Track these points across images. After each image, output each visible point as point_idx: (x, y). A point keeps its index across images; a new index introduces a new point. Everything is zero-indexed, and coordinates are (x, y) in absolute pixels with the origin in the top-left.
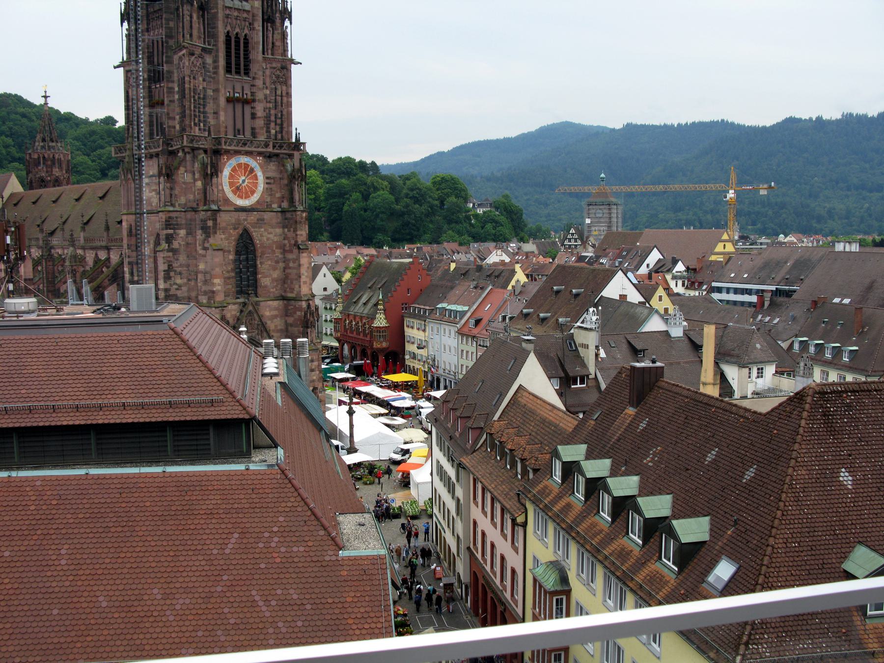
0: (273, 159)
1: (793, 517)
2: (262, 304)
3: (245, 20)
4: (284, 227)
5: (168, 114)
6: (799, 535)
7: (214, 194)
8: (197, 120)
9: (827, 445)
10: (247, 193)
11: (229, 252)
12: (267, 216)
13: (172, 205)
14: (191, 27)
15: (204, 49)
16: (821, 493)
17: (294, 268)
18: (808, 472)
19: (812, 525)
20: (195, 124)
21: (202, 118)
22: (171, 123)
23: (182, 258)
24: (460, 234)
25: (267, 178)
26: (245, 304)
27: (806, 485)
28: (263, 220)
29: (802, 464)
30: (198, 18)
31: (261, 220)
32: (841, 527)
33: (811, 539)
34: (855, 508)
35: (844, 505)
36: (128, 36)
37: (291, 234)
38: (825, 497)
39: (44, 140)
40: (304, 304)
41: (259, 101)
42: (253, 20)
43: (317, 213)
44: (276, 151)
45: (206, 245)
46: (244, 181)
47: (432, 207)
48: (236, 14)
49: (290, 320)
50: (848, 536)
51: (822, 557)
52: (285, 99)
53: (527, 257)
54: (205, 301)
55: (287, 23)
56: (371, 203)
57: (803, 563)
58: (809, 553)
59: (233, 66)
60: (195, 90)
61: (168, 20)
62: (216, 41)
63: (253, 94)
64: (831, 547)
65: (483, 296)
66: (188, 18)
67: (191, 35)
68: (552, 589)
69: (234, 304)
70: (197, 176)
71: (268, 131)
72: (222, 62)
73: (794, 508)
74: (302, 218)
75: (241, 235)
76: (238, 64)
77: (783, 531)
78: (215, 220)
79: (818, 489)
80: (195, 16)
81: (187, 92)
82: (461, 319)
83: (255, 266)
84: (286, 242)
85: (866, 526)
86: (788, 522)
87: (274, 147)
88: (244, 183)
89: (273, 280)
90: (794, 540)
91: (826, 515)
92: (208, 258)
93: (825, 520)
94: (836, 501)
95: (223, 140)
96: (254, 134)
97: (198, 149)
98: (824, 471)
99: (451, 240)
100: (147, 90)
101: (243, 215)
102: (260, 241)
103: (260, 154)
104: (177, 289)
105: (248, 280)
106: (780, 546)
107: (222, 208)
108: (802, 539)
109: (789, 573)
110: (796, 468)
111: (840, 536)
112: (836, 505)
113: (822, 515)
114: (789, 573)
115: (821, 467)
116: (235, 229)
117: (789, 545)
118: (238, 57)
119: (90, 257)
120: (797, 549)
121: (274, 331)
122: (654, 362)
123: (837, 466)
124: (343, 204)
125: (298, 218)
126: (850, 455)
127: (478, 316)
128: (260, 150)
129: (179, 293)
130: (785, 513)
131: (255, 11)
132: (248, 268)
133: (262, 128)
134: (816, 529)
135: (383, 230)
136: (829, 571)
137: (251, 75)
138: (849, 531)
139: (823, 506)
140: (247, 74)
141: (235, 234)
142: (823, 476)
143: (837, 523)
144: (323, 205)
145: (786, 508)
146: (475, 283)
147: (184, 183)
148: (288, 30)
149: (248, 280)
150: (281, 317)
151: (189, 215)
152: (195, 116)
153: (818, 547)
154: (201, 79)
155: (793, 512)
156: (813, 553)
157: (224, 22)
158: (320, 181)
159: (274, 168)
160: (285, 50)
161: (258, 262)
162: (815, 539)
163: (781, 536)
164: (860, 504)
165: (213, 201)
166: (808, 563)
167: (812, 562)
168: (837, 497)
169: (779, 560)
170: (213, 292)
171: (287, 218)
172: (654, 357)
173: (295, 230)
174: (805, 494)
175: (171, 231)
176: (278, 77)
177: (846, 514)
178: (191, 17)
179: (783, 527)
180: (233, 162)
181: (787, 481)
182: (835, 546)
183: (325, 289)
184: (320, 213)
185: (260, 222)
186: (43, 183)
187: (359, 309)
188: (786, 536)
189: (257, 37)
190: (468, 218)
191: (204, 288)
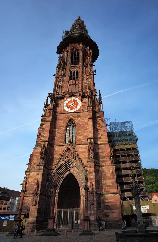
74: (90, 109)
89: (84, 137)
102: (78, 122)
116: (67, 119)
121: (83, 158)
137: (79, 78)
141: (67, 121)
161: (77, 130)
180: (69, 99)
185: (78, 116)
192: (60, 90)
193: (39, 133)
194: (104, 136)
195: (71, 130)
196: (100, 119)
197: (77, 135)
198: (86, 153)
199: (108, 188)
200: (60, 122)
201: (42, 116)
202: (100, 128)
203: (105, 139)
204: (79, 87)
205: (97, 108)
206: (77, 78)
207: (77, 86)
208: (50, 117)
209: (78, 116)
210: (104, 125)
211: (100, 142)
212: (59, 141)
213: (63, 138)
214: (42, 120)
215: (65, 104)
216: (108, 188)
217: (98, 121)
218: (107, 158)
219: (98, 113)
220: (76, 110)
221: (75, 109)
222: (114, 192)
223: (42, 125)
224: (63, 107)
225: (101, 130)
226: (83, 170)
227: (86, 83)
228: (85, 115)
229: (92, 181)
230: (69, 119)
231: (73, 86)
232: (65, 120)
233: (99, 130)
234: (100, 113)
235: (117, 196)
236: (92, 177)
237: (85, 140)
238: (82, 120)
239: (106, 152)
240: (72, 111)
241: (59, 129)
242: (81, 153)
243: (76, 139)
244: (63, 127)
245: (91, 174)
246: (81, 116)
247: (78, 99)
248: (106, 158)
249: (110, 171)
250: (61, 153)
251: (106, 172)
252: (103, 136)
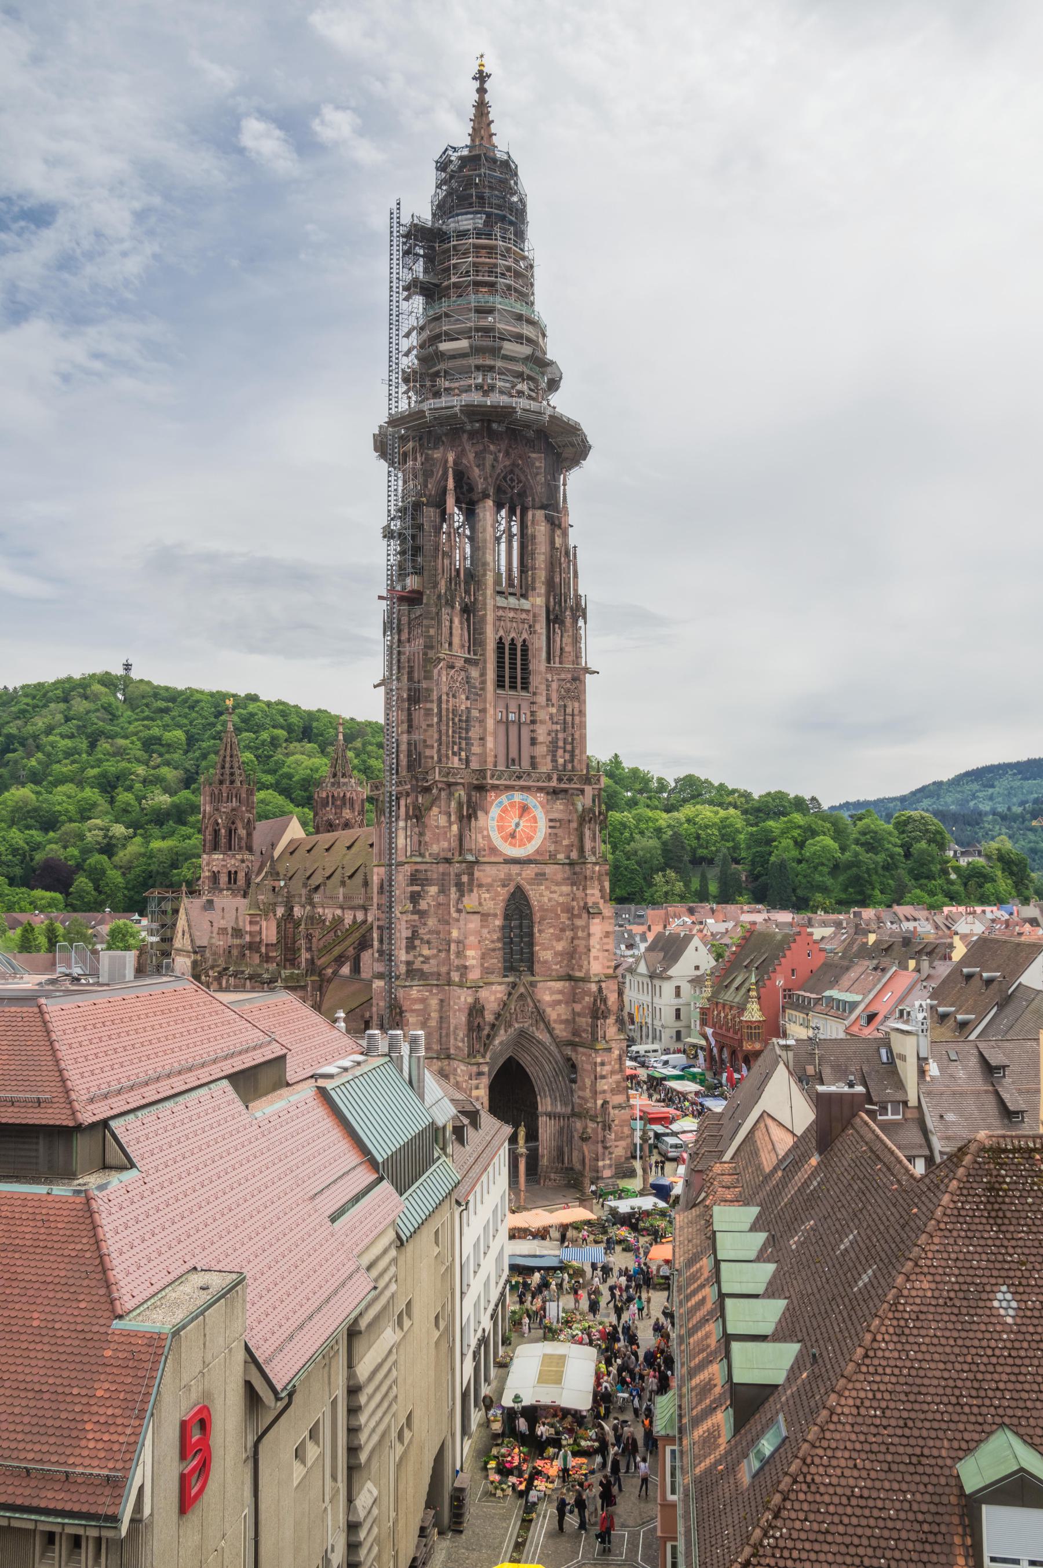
1: (884, 1363)
2: (540, 985)
3: (523, 621)
4: (573, 884)
5: (425, 741)
6: (887, 1396)
7: (476, 840)
8: (456, 748)
9: (982, 1242)
10: (521, 840)
11: (495, 915)
12: (549, 870)
13: (421, 855)
14: (451, 634)
15: (467, 661)
16: (950, 1326)
17: (583, 938)
18: (933, 1286)
19: (918, 1381)
20: (454, 754)
21: (463, 745)
22: (428, 752)
23: (432, 922)
24: (932, 893)
25: (551, 820)
26: (514, 985)
27: (924, 1309)
28: (544, 874)
29: (926, 1270)
30: (461, 623)
31: (541, 876)
32: (974, 1393)
33: (909, 1406)
34: (1010, 1361)
35: (989, 1352)
36: (390, 648)
37: (579, 894)
38: (955, 1334)
39: (335, 775)
40: (594, 987)
41: (542, 722)
42: (535, 621)
43: (734, 866)
44: (563, 786)
45: (460, 906)
46: (517, 825)
47: (892, 856)
48: (512, 614)
49: (578, 1008)
50: (984, 1410)
51: (921, 1442)
52: (577, 719)
53: (1007, 927)
54: (457, 979)
55: (581, 623)
56: (807, 853)
57: (883, 1448)
58: (899, 1432)
59: (507, 679)
60: (454, 711)
61: (428, 627)
62: (484, 650)
63: (533, 713)
64: (944, 1426)
65: (884, 980)
66: (448, 623)
67: (450, 644)
68: (663, 1433)
69: (500, 984)
70: (453, 818)
71: (554, 760)
72: (491, 675)
73: (891, 1346)
74: (594, 872)
75: (513, 894)
76: (513, 678)
77: (858, 1385)
78: (471, 874)
79: (946, 1318)
80: (456, 621)
81: (444, 713)
82: (851, 1012)
83: (531, 935)
84: (575, 903)
85: (1025, 1395)
86: (872, 1369)
87: (560, 780)
88: (517, 827)
89: (556, 954)
90: (875, 1404)
91: (949, 1366)
92: (462, 922)
93: (946, 1375)
94: (976, 1343)
95: (489, 773)
96: (534, 765)
97: (457, 784)
98: (965, 1287)
99: (916, 902)
100: (405, 713)
101: (515, 869)
103: (540, 789)
105: (522, 954)
106: (846, 1410)
107: (482, 859)
108: (892, 1405)
109: (851, 1464)
110: (913, 1277)
111: (967, 1409)
112: (973, 1351)
113: (941, 1366)
114: (851, 1464)
115: (961, 1279)
116: (504, 886)
117: (863, 1411)
118: (513, 668)
119: (348, 919)
120: (877, 1422)
121: (555, 1021)
122: (851, 1085)
123: (993, 1281)
124: (770, 854)
125: (588, 873)
126: (1023, 1264)
127: (872, 1009)
128: (540, 784)
129: (426, 968)
130: (871, 1353)
131: (537, 611)
132: (521, 937)
133: (544, 757)
134: (924, 1390)
135: (824, 890)
136: (929, 1470)
137: (531, 690)
138: (987, 1402)
139: (948, 1350)
140: (525, 687)
141: (504, 893)
142: (961, 1295)
143: (968, 1384)
144: (743, 854)
145: (875, 1345)
146: (875, 962)
147: (437, 827)
148: (582, 632)
149: (522, 954)
150: (567, 1003)
151: (442, 868)
152: (454, 743)
153: (919, 1424)
154: (463, 697)
155: (887, 1354)
156: (907, 1432)
157: (494, 625)
158: (740, 824)
160: (578, 656)
161: (536, 930)
162: (917, 1407)
163: (854, 1394)
164: (1023, 1353)
165: (470, 850)
166: (892, 1449)
167: (901, 1450)
168: (980, 1335)
169: (837, 1436)
170: (466, 967)
171: (576, 871)
172: (852, 1078)
173: (585, 889)
174: (918, 1324)
175: (417, 888)
176: (568, 691)
177: (991, 1368)
178: (451, 622)
179: (861, 1377)
181: (890, 1297)
182: (952, 1426)
183: (697, 968)
184: (739, 867)
185: (541, 876)
186: (330, 827)
187: (729, 996)
188: (862, 1394)
189: (539, 643)
190: (945, 872)
191: (457, 962)
244: (495, 915)
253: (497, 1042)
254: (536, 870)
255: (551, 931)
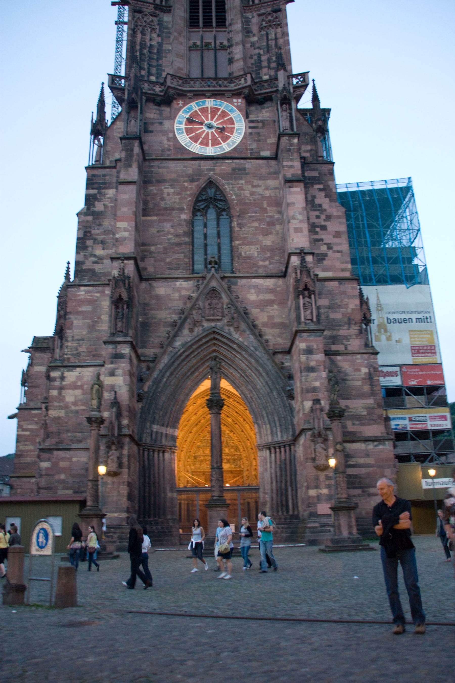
0: (266, 105)
28: (244, 169)
52: (281, 41)
63: (229, 40)
74: (291, 144)
89: (263, 249)
104: (94, 262)
116: (192, 181)
121: (265, 325)
129: (98, 268)
137: (227, 23)
141: (192, 188)
154: (154, 35)
159: (268, 114)
161: (235, 224)
180: (194, 106)
185: (238, 173)
192: (153, 66)
193: (82, 232)
194: (338, 252)
195: (212, 225)
196: (320, 190)
197: (237, 243)
198: (276, 307)
199: (354, 424)
200: (166, 191)
201: (87, 165)
202: (323, 223)
203: (342, 263)
204: (231, 61)
205: (309, 147)
206: (222, 22)
207: (223, 57)
208: (130, 169)
209: (237, 172)
210: (338, 211)
211: (324, 270)
212: (168, 260)
213: (183, 253)
214: (90, 183)
215: (180, 123)
216: (354, 424)
217: (314, 197)
218: (349, 328)
219: (312, 167)
220: (226, 147)
221: (224, 145)
222: (375, 437)
223: (90, 200)
224: (171, 135)
225: (324, 228)
226: (269, 365)
227: (257, 45)
228: (264, 171)
229: (318, 396)
230: (202, 182)
231: (205, 52)
232: (186, 184)
233: (318, 229)
234: (319, 167)
235: (384, 447)
236: (317, 384)
237: (267, 263)
238: (254, 186)
239: (347, 306)
240: (210, 151)
241: (162, 218)
242: (257, 306)
243: (236, 259)
244: (181, 210)
245: (313, 375)
246: (248, 174)
247: (233, 110)
248: (346, 327)
249: (359, 370)
250: (179, 305)
251: (346, 374)
252: (334, 251)
253: (178, 343)
254: (234, 165)
255: (256, 224)
